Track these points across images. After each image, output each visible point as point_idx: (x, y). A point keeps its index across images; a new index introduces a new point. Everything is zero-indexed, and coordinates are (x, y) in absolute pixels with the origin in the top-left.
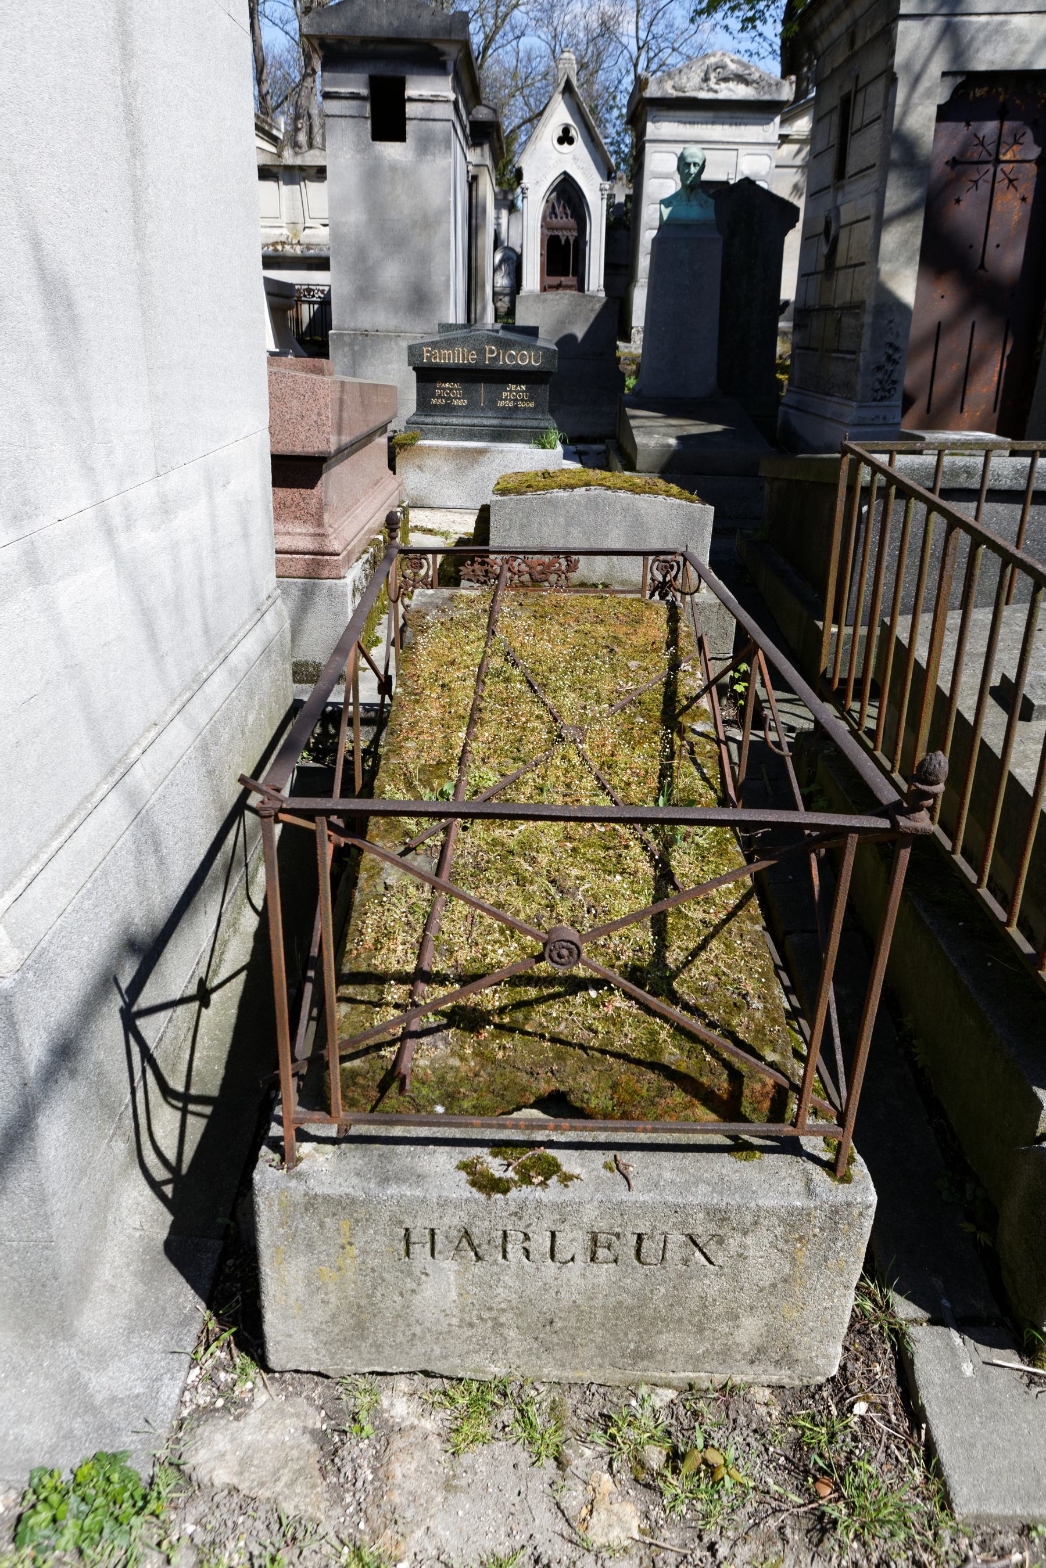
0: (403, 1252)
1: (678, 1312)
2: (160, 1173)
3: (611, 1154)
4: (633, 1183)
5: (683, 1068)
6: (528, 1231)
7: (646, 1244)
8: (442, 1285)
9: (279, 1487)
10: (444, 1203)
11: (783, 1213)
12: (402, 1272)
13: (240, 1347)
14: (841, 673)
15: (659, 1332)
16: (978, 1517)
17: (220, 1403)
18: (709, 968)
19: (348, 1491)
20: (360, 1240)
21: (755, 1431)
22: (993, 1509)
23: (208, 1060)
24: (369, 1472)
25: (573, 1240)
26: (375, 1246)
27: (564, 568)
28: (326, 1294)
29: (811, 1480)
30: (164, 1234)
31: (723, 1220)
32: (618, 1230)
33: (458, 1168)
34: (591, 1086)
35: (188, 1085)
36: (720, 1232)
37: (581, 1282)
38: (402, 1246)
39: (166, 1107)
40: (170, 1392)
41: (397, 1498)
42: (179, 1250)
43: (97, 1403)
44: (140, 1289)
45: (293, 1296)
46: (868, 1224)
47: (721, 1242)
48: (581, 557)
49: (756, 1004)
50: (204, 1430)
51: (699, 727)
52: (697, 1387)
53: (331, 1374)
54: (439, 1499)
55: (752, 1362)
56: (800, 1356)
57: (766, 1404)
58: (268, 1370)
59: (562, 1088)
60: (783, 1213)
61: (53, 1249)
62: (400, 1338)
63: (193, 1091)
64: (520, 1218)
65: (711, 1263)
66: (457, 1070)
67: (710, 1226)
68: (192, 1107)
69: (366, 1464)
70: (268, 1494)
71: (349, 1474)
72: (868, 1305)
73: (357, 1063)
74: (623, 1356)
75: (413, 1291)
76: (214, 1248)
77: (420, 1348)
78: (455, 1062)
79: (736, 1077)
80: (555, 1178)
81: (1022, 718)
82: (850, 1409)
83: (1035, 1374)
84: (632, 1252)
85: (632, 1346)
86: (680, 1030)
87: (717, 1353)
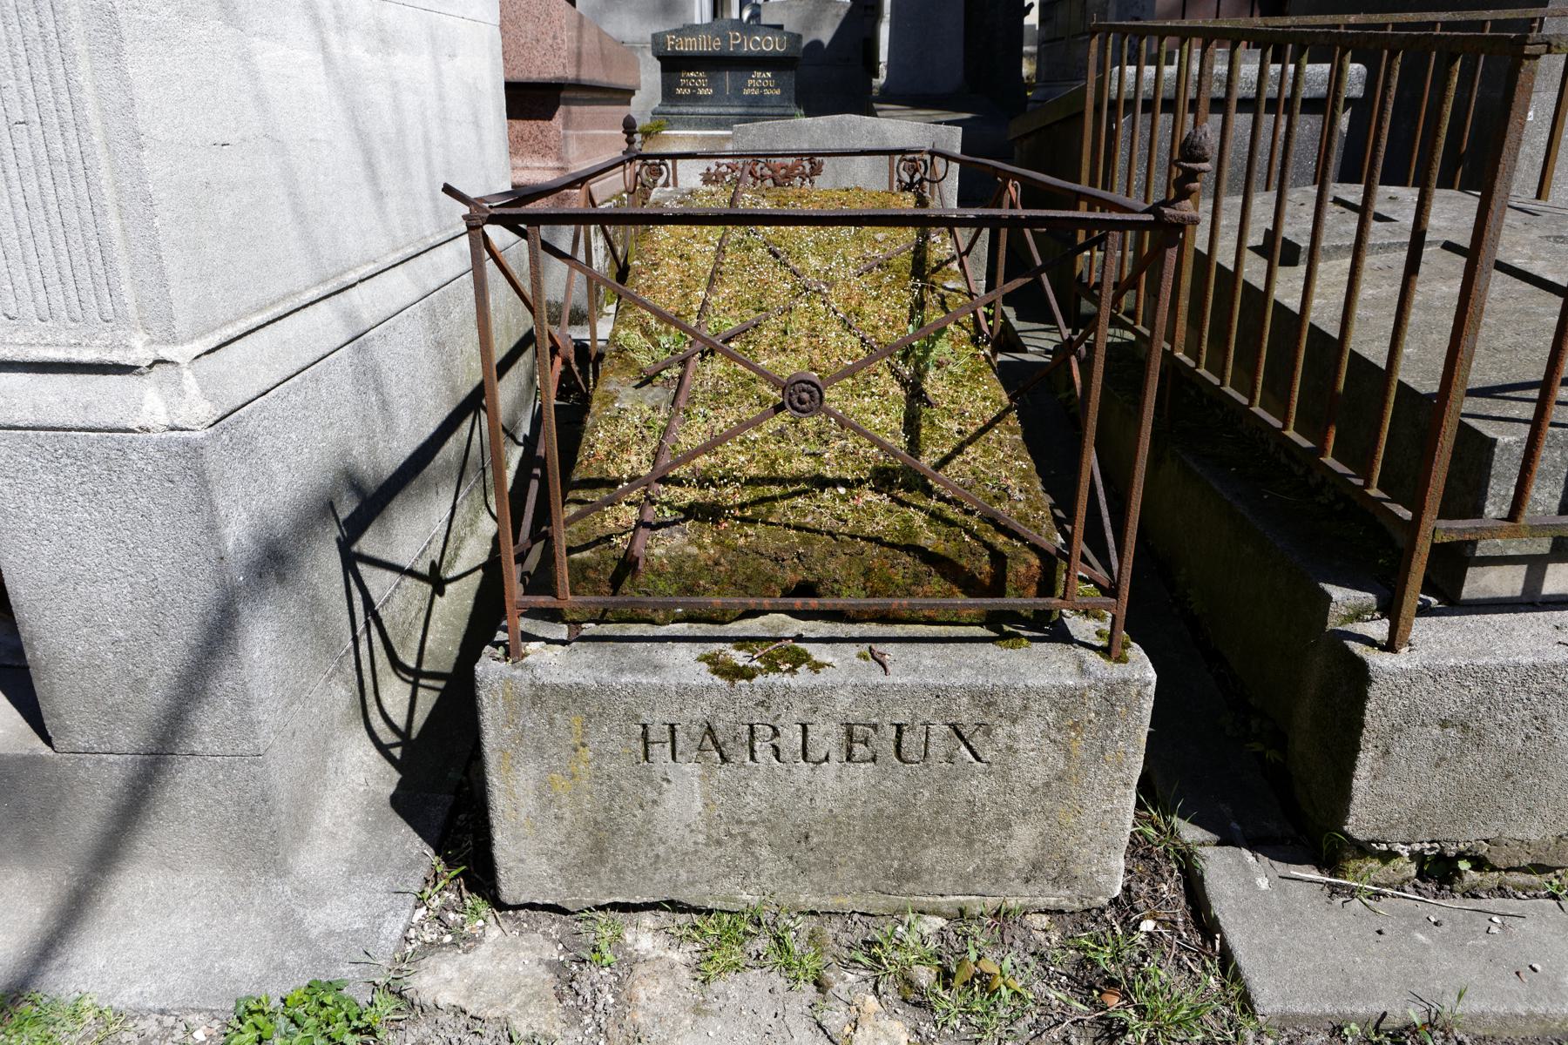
0: (641, 755)
1: (945, 820)
2: (387, 737)
3: (866, 646)
4: (890, 668)
5: (941, 549)
6: (777, 724)
7: (906, 737)
8: (685, 795)
9: (510, 1008)
10: (684, 692)
11: (1055, 696)
12: (641, 778)
13: (470, 889)
14: (1095, 277)
15: (925, 847)
16: (1283, 1017)
17: (448, 938)
18: (966, 468)
19: (587, 1013)
20: (594, 741)
21: (1033, 954)
22: (1299, 1007)
23: (441, 643)
24: (609, 997)
25: (827, 734)
26: (610, 747)
27: (807, 170)
28: (560, 808)
29: (1096, 993)
30: (392, 790)
31: (989, 704)
32: (875, 720)
33: (699, 660)
34: (841, 574)
35: (420, 661)
36: (986, 720)
37: (838, 787)
38: (640, 745)
39: (395, 678)
40: (393, 928)
41: (640, 1017)
42: (405, 804)
43: (312, 937)
44: (363, 836)
45: (524, 811)
46: (1148, 706)
47: (988, 733)
48: (826, 160)
49: (1017, 495)
50: (430, 961)
51: (950, 285)
52: (968, 913)
53: (569, 907)
54: (688, 1022)
55: (1027, 881)
56: (1079, 871)
57: (1045, 931)
58: (499, 905)
59: (811, 578)
60: (1055, 696)
61: (261, 764)
62: (642, 861)
63: (425, 668)
64: (768, 708)
65: (978, 759)
66: (695, 558)
67: (976, 712)
68: (422, 682)
69: (606, 988)
70: (498, 1014)
71: (588, 996)
72: (1151, 831)
73: (586, 554)
74: (886, 877)
75: (654, 802)
76: (442, 788)
77: (664, 873)
78: (694, 550)
79: (998, 558)
80: (805, 666)
81: (1283, 263)
82: (1136, 928)
83: (1337, 885)
84: (892, 747)
85: (896, 864)
86: (935, 516)
87: (989, 871)
